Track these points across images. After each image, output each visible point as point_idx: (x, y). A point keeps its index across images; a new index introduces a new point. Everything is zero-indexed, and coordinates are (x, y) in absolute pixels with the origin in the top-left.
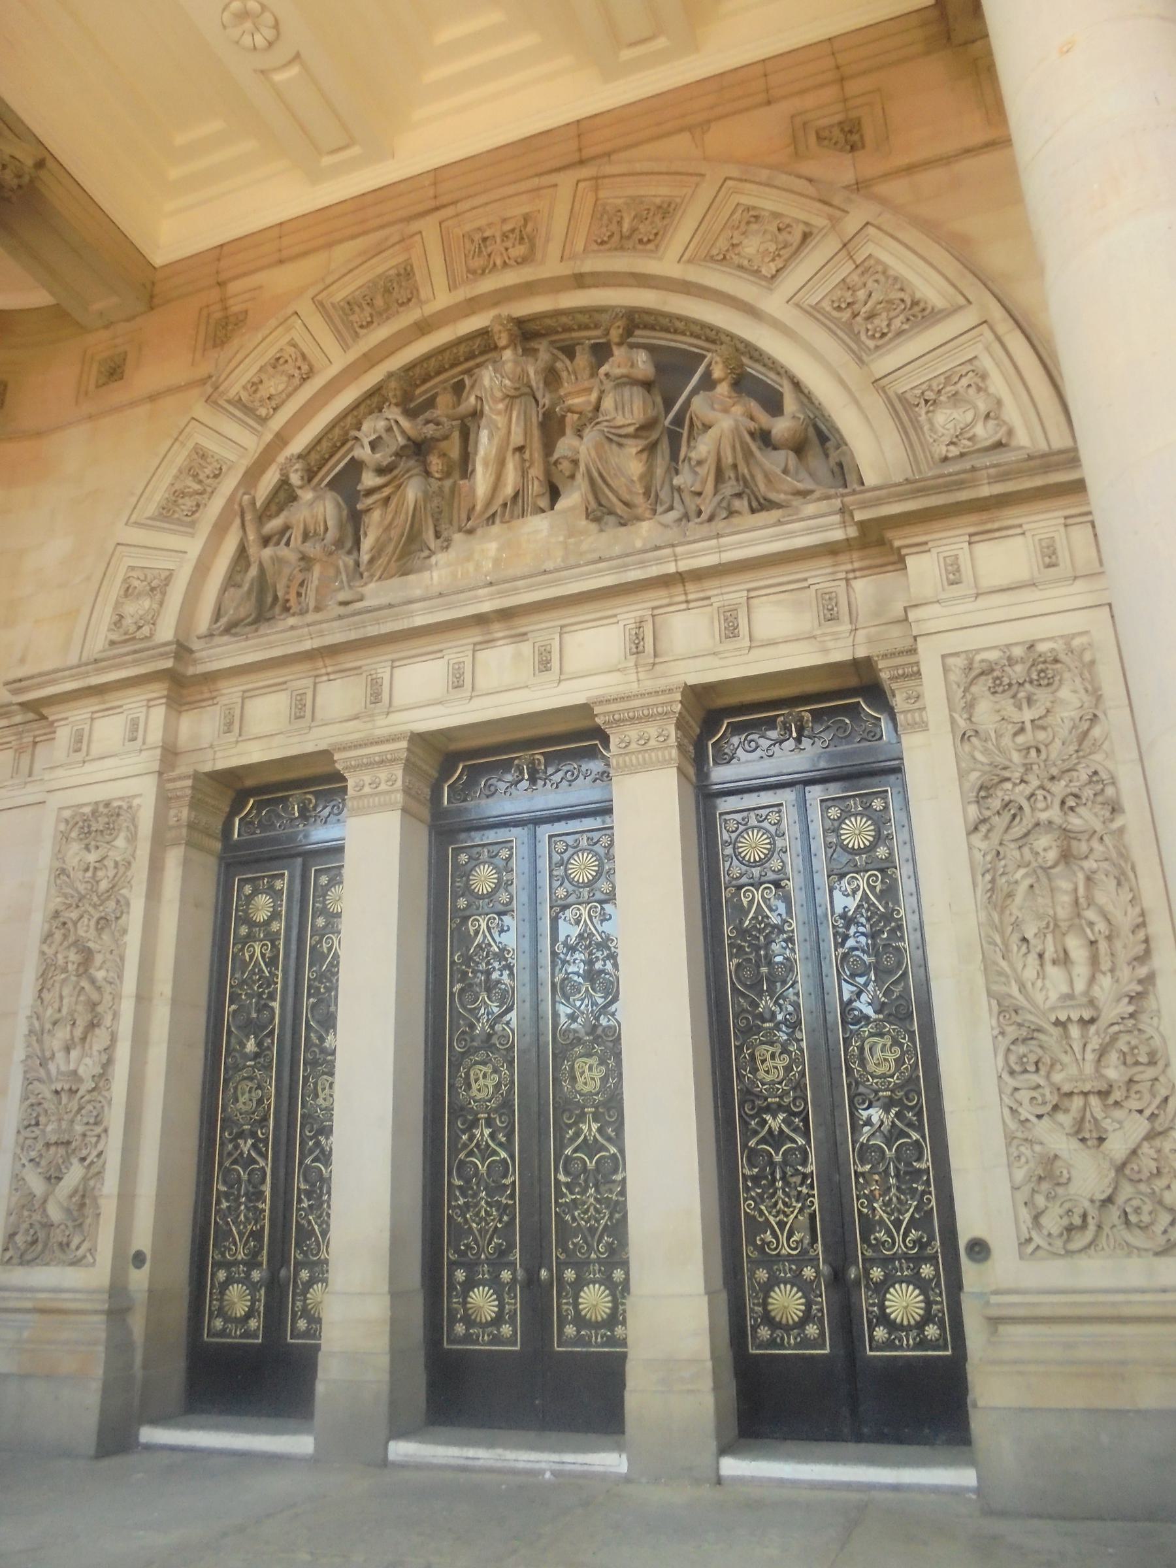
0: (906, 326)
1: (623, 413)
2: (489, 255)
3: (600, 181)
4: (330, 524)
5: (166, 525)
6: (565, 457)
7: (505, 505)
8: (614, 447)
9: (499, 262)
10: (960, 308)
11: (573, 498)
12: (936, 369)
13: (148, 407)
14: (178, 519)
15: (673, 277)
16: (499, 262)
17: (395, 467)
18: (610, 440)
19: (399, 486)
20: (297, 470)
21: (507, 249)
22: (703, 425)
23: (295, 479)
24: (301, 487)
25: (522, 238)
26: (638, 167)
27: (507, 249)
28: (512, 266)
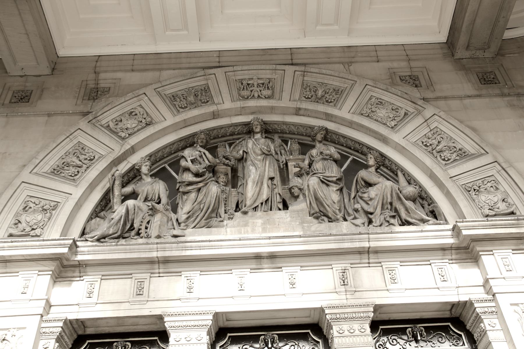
0: (457, 158)
1: (329, 171)
2: (251, 91)
3: (306, 73)
4: (161, 196)
5: (56, 178)
6: (297, 186)
7: (262, 204)
8: (324, 186)
9: (256, 95)
10: (482, 154)
11: (300, 206)
12: (476, 177)
13: (46, 118)
14: (63, 176)
15: (347, 116)
16: (256, 95)
17: (204, 175)
18: (323, 182)
19: (206, 184)
20: (146, 165)
21: (261, 91)
22: (366, 182)
23: (144, 169)
24: (146, 175)
25: (268, 88)
26: (324, 71)
27: (261, 91)
28: (262, 98)
